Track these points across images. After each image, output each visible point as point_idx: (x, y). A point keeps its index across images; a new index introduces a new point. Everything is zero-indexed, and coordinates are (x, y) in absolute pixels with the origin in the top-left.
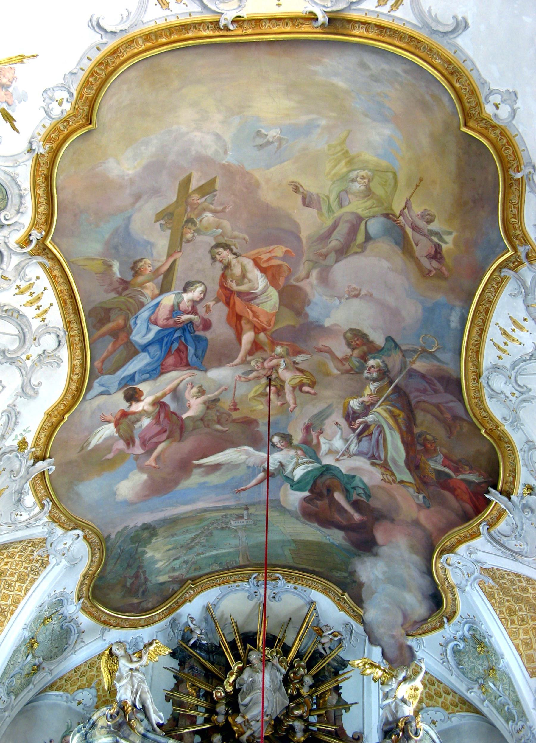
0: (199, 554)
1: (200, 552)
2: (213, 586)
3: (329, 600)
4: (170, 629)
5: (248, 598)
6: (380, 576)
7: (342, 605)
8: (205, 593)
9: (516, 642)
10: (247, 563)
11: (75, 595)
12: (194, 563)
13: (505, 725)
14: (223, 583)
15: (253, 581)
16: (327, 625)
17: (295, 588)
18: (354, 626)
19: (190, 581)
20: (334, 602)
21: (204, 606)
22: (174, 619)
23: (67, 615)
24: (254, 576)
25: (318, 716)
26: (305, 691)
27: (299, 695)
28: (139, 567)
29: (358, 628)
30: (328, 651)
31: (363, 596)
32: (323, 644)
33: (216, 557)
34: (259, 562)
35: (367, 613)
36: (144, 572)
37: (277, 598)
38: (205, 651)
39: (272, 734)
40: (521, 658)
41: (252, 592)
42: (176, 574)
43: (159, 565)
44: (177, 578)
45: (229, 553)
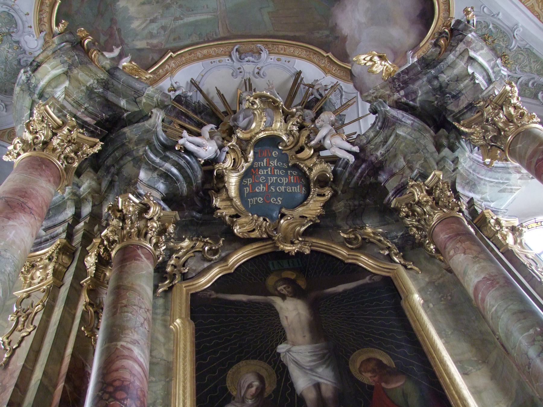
0: (176, 19)
1: (178, 14)
2: (194, 61)
6: (363, 20)
9: (529, 4)
10: (227, 35)
11: (32, 20)
12: (173, 31)
13: (534, 101)
14: (205, 57)
15: (235, 55)
17: (279, 60)
18: (343, 87)
21: (187, 83)
23: (26, 48)
24: (236, 47)
28: (113, 21)
31: (348, 51)
33: (195, 24)
34: (239, 33)
36: (119, 30)
37: (261, 73)
40: (539, 19)
42: (155, 41)
43: (135, 24)
44: (156, 47)
45: (208, 20)
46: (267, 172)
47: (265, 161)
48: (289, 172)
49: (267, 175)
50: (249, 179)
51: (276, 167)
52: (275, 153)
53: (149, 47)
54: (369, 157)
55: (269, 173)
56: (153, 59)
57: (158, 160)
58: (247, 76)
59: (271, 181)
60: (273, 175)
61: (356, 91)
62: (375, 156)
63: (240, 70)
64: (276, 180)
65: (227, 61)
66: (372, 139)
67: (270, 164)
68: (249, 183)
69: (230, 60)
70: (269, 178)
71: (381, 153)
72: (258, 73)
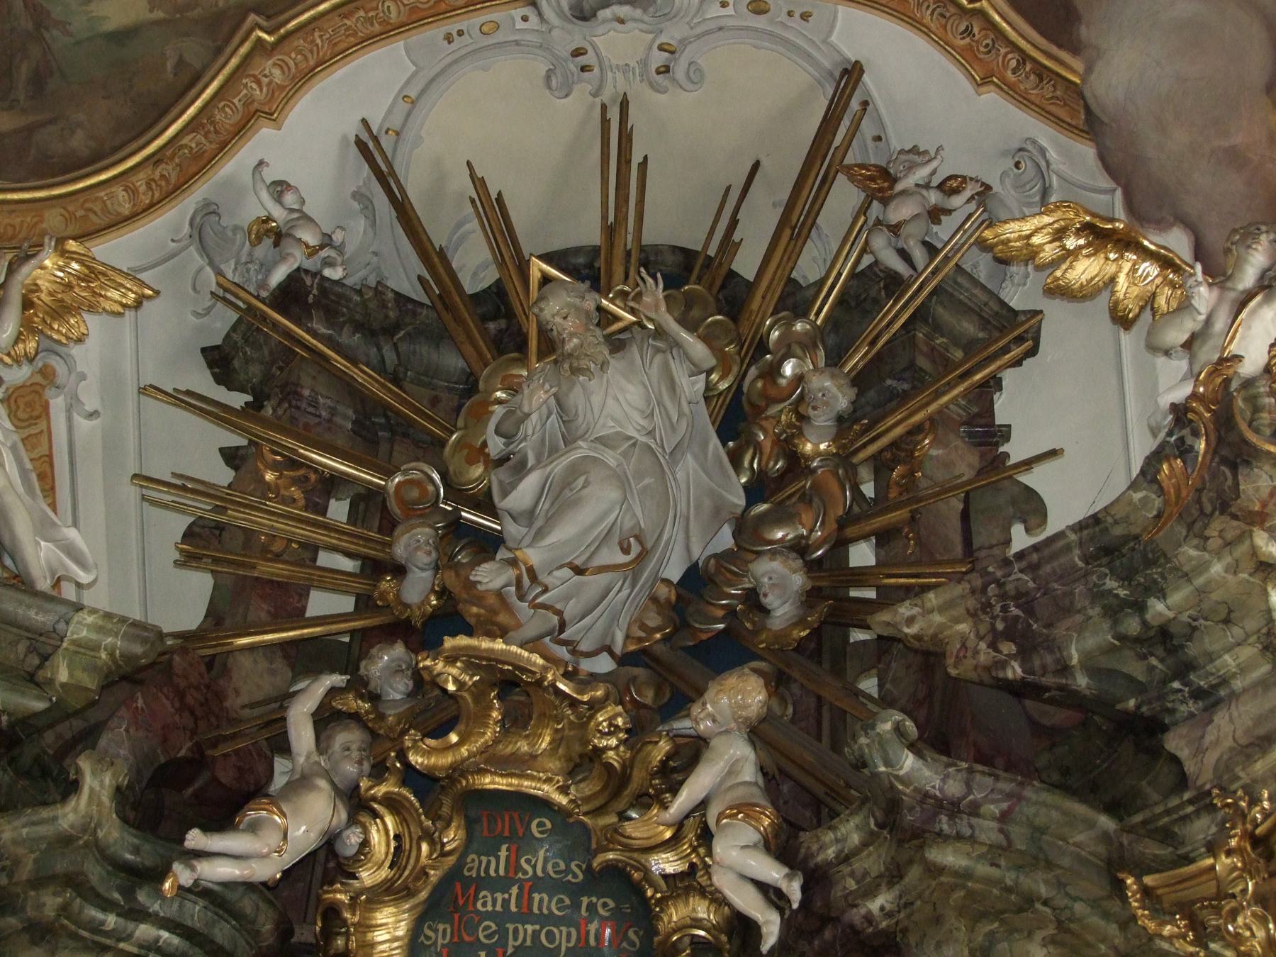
3: (920, 43)
4: (195, 258)
5: (548, 78)
7: (982, 58)
8: (341, 73)
16: (914, 150)
18: (1052, 154)
19: (252, 18)
20: (944, 45)
21: (345, 138)
22: (209, 210)
25: (883, 538)
26: (816, 445)
27: (796, 464)
29: (1073, 159)
30: (919, 255)
32: (895, 229)
35: (1099, 66)
37: (679, 71)
38: (359, 327)
39: (666, 639)
41: (566, 54)
46: (506, 903)
47: (503, 853)
48: (585, 900)
49: (502, 917)
50: (441, 927)
51: (538, 883)
52: (540, 825)
53: (159, 14)
54: (844, 912)
55: (513, 908)
56: (181, 63)
57: (111, 920)
58: (615, 85)
59: (516, 939)
60: (525, 916)
61: (1112, 185)
62: (863, 911)
63: (582, 60)
64: (536, 935)
65: (520, 25)
66: (855, 852)
67: (518, 868)
68: (440, 941)
69: (534, 19)
70: (511, 927)
71: (882, 908)
72: (665, 70)
